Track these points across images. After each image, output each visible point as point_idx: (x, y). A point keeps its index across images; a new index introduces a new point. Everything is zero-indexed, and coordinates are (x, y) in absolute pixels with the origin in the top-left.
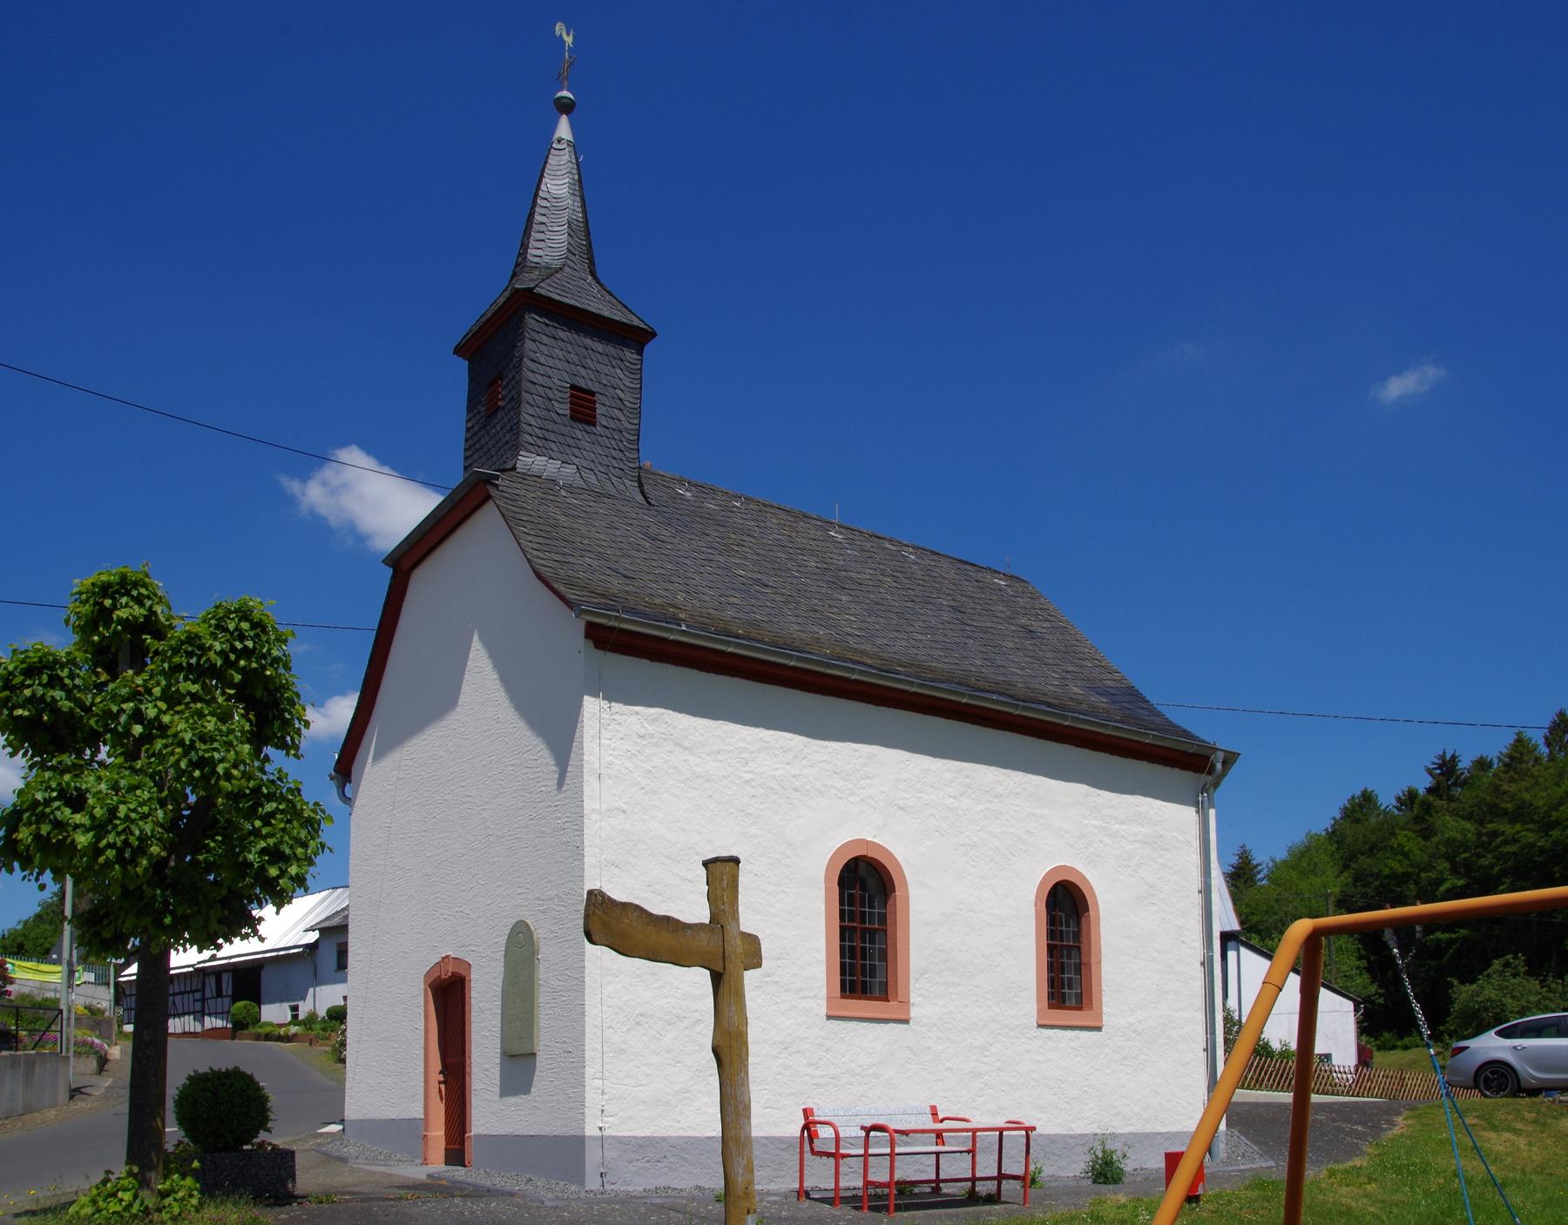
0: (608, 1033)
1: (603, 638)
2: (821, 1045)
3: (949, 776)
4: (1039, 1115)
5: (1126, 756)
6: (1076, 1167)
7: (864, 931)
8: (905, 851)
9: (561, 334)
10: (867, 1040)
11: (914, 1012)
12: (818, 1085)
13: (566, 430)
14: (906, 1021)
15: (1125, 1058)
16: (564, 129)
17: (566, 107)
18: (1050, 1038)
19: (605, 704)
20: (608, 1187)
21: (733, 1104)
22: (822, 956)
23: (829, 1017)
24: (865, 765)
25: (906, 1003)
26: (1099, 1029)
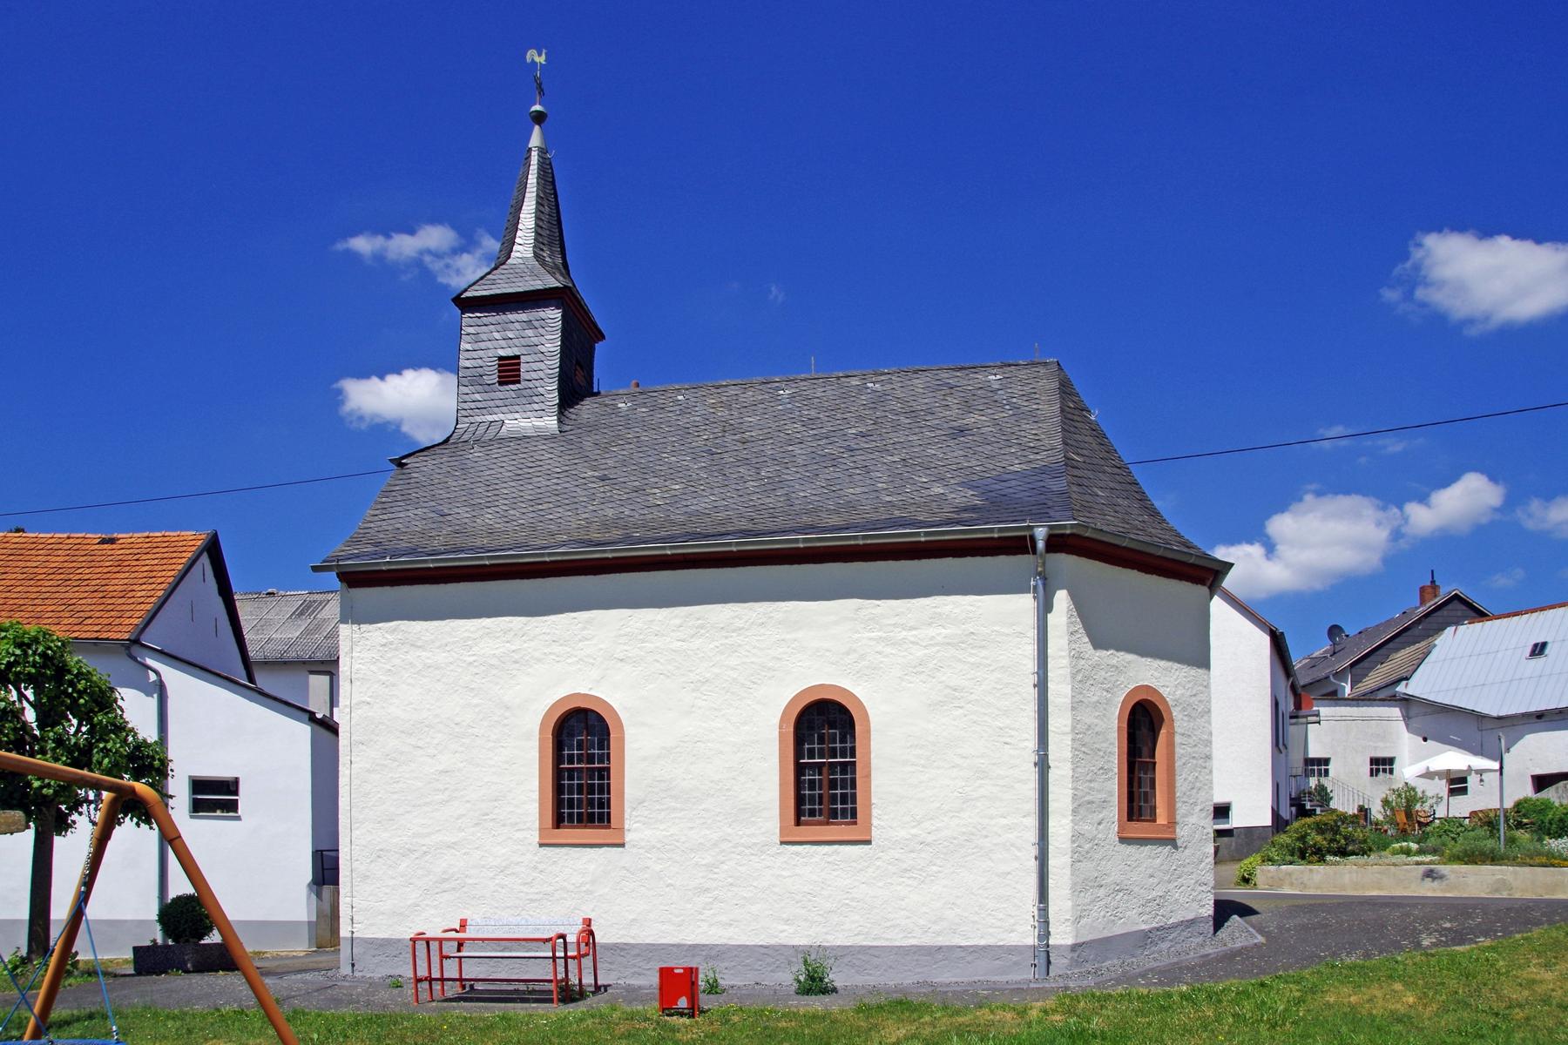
0: (355, 865)
1: (354, 579)
2: (535, 868)
3: (677, 622)
4: (781, 927)
5: (919, 558)
6: (787, 978)
7: (600, 770)
8: (612, 692)
9: (491, 319)
10: (823, 865)
11: (628, 837)
12: (532, 900)
13: (500, 395)
14: (622, 845)
15: (906, 870)
16: (535, 140)
17: (539, 118)
18: (797, 854)
19: (355, 627)
20: (357, 974)
21: (1045, 934)
22: (536, 795)
23: (541, 845)
24: (584, 629)
25: (621, 829)
26: (868, 842)
